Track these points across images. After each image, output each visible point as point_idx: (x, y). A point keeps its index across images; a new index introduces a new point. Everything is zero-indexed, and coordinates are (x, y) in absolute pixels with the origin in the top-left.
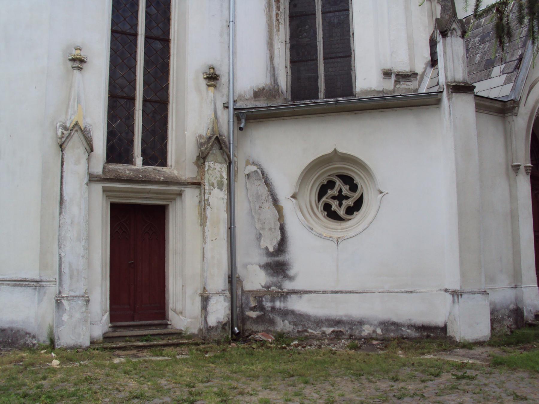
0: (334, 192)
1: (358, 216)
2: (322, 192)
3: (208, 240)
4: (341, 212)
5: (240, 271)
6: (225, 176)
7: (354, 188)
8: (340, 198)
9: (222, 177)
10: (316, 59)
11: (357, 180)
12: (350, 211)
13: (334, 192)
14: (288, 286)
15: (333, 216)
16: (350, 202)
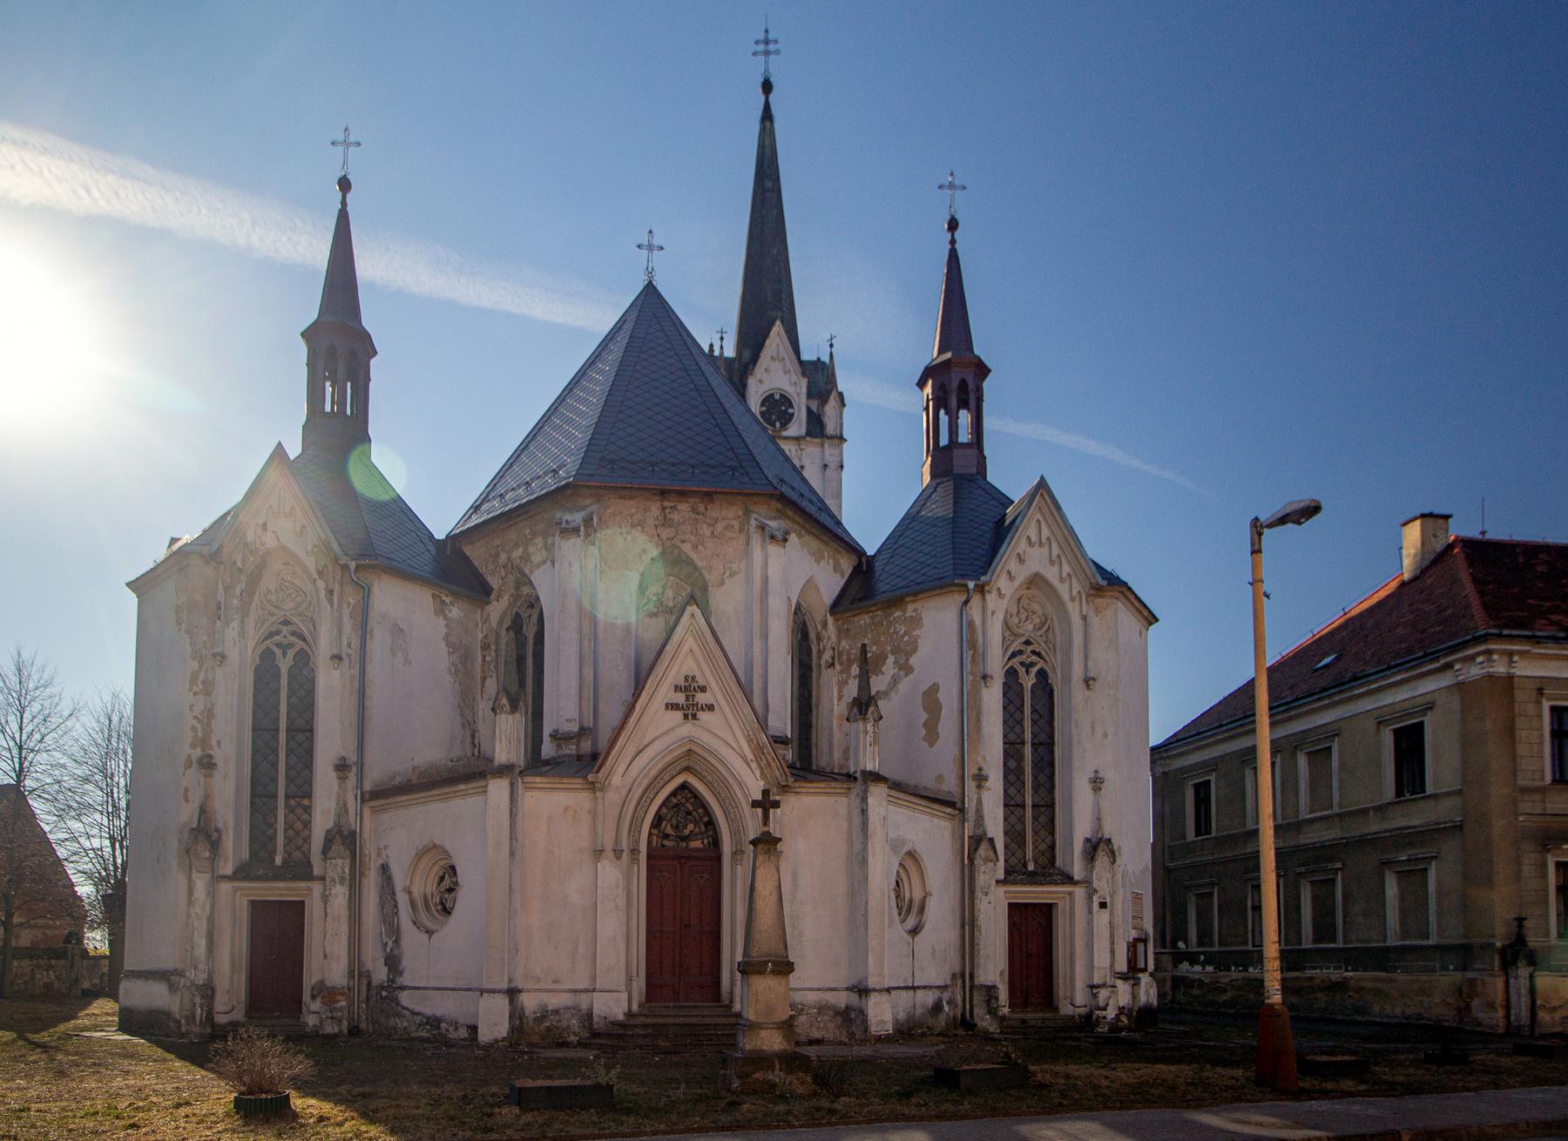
9: (344, 872)
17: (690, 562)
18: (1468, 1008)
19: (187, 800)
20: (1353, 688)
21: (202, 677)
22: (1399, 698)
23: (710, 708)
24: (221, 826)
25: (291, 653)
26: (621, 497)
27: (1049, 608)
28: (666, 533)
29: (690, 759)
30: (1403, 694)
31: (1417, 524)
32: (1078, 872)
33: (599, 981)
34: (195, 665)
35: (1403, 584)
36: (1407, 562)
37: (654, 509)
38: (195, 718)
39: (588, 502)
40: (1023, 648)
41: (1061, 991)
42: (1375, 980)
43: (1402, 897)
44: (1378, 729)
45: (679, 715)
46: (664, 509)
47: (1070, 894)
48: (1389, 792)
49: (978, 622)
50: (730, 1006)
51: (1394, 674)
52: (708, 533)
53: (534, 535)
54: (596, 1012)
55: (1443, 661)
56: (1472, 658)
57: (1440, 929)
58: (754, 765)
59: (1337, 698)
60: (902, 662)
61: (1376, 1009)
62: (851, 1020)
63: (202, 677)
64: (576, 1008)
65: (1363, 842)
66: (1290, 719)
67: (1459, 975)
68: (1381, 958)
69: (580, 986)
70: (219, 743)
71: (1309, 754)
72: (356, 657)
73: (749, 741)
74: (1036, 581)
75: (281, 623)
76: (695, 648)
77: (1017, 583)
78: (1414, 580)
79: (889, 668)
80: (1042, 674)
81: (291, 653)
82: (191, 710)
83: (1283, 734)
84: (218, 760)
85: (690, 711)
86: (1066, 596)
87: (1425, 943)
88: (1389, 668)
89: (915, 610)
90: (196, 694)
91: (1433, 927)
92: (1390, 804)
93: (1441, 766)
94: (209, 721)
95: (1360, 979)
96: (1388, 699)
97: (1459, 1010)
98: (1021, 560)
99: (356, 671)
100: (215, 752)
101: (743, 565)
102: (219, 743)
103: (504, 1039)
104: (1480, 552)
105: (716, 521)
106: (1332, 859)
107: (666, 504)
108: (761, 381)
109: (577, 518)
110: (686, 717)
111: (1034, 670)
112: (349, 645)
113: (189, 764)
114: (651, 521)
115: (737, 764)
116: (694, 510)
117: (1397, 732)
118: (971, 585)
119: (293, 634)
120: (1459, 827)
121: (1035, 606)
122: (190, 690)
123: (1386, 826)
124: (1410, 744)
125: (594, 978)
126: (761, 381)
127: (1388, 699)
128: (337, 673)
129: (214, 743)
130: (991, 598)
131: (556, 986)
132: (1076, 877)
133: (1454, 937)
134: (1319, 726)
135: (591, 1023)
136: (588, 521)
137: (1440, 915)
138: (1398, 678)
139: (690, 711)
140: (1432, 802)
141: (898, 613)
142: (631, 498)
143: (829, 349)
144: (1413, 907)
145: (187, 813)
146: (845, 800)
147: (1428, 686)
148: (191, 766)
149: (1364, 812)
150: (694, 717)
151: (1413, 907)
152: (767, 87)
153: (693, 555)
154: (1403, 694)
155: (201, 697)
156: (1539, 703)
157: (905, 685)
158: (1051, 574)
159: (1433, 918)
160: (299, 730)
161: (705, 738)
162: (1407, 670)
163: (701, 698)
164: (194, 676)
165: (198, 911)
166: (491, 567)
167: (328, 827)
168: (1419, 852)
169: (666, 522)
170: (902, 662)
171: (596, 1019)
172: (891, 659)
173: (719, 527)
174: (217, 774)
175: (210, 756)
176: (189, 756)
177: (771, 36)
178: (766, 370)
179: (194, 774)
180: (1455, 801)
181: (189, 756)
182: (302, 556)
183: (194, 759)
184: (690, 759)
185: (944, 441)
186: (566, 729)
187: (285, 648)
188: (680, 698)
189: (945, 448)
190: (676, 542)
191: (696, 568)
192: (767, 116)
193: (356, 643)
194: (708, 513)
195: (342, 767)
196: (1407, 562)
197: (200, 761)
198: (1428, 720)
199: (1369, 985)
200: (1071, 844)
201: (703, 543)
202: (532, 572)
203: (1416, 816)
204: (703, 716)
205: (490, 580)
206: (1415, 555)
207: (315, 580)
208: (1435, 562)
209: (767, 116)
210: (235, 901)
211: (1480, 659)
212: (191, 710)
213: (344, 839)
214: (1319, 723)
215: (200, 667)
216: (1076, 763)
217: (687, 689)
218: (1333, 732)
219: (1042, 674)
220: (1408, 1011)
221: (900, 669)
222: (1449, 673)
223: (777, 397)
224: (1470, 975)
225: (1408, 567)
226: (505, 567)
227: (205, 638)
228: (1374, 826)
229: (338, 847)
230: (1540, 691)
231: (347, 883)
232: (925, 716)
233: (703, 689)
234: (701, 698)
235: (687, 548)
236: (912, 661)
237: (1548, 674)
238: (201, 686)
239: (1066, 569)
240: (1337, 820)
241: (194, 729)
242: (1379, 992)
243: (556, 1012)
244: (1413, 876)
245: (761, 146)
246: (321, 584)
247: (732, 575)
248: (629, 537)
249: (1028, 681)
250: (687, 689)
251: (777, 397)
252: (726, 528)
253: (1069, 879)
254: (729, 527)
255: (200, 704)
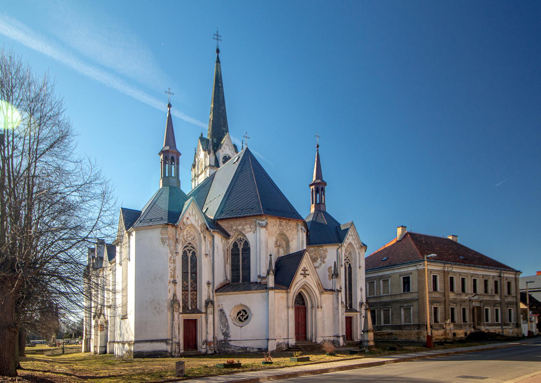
0: (241, 314)
1: (247, 320)
2: (238, 314)
3: (208, 328)
4: (243, 319)
5: (216, 335)
6: (212, 311)
7: (246, 313)
8: (243, 316)
10: (239, 270)
11: (247, 311)
12: (245, 319)
13: (241, 314)
14: (229, 339)
15: (241, 320)
16: (245, 317)
17: (285, 235)
18: (420, 337)
19: (170, 292)
20: (395, 267)
21: (172, 258)
22: (404, 271)
23: (308, 275)
24: (179, 299)
25: (191, 252)
26: (272, 218)
27: (351, 250)
28: (281, 228)
29: (305, 287)
30: (405, 270)
31: (401, 228)
32: (358, 309)
33: (289, 336)
34: (170, 255)
35: (397, 241)
36: (398, 236)
37: (278, 222)
38: (171, 270)
39: (264, 219)
40: (346, 258)
41: (354, 335)
42: (399, 332)
43: (405, 314)
44: (400, 277)
45: (303, 276)
46: (280, 222)
47: (356, 314)
48: (402, 291)
49: (340, 253)
50: (311, 340)
51: (404, 265)
52: (289, 229)
53: (247, 224)
54: (289, 343)
55: (415, 264)
56: (421, 265)
57: (414, 321)
58: (317, 288)
59: (391, 269)
60: (322, 260)
61: (399, 338)
62: (334, 343)
63: (172, 258)
64: (285, 343)
65: (397, 302)
66: (379, 272)
67: (417, 331)
68: (400, 327)
69: (285, 338)
70: (177, 276)
71: (383, 281)
72: (211, 255)
73: (316, 282)
74: (350, 244)
75: (188, 244)
76: (306, 261)
77: (347, 244)
78: (400, 241)
79: (319, 261)
80: (350, 265)
81: (191, 252)
82: (170, 267)
83: (377, 275)
84: (177, 281)
85: (305, 275)
86: (355, 248)
87: (410, 324)
88: (403, 264)
89: (326, 248)
90: (171, 263)
91: (412, 321)
92: (402, 293)
93: (414, 286)
94: (175, 271)
95: (395, 332)
96: (402, 270)
97: (418, 338)
98: (348, 239)
99: (211, 258)
100: (176, 279)
101: (296, 236)
102: (177, 276)
103: (275, 350)
104: (413, 236)
105: (291, 226)
106: (389, 305)
107: (281, 221)
108: (223, 151)
109: (264, 223)
110: (304, 276)
111: (348, 263)
112: (209, 251)
113: (170, 282)
114: (277, 225)
115: (314, 287)
116: (286, 223)
117: (403, 278)
118: (340, 244)
119: (191, 247)
120: (418, 300)
121: (348, 249)
122: (170, 262)
123: (402, 298)
124: (407, 281)
125: (288, 335)
126: (223, 151)
127: (402, 270)
128: (206, 259)
129: (176, 277)
130: (343, 247)
131: (280, 338)
132: (358, 311)
133: (417, 322)
134: (386, 275)
135: (288, 346)
136: (267, 224)
137: (413, 318)
138: (405, 266)
139: (305, 275)
140: (411, 294)
141: (321, 248)
142: (273, 218)
143: (242, 144)
144: (407, 316)
145: (170, 296)
146: (332, 295)
147: (411, 269)
148: (170, 283)
149: (397, 295)
150: (306, 277)
151: (407, 316)
152: (218, 51)
153: (286, 233)
154: (405, 270)
155: (172, 264)
156: (431, 275)
157: (323, 265)
158: (353, 242)
159: (412, 318)
160: (193, 273)
161: (308, 282)
162: (407, 265)
163: (307, 272)
164: (171, 258)
165: (176, 322)
166: (229, 229)
167: (206, 299)
168: (409, 304)
169: (280, 225)
170: (322, 260)
171: (289, 345)
172: (319, 259)
173: (291, 227)
174: (177, 285)
175: (175, 280)
176: (170, 280)
177: (219, 34)
178: (224, 148)
179: (171, 285)
180: (416, 294)
181: (170, 280)
182: (196, 226)
183: (171, 281)
184: (305, 287)
185: (318, 202)
186: (263, 276)
187: (190, 250)
188: (303, 272)
189: (318, 204)
190: (283, 230)
191: (286, 236)
192: (218, 61)
193: (211, 251)
194: (289, 223)
195: (208, 284)
196: (398, 236)
197: (173, 282)
198: (411, 276)
199: (398, 333)
200: (357, 303)
201: (288, 231)
202: (246, 233)
203: (408, 297)
204: (307, 276)
205: (229, 233)
206: (400, 235)
207: (200, 234)
208: (404, 237)
209: (218, 61)
210: (180, 318)
211: (422, 265)
212: (170, 267)
213: (209, 302)
214: (386, 274)
215: (172, 256)
216: (358, 285)
217: (304, 270)
218: (389, 276)
219: (350, 265)
220: (407, 339)
221: (322, 261)
222: (416, 267)
223: (227, 157)
224: (420, 330)
225: (398, 237)
226: (235, 230)
227: (173, 248)
228: (399, 298)
229: (210, 305)
230: (431, 272)
231: (213, 314)
232: (328, 273)
233: (307, 270)
234: (307, 272)
235: (285, 232)
236: (325, 260)
237: (432, 268)
238: (172, 261)
239: (356, 242)
240: (390, 296)
241: (171, 273)
242: (400, 335)
243: (281, 344)
244: (408, 309)
245: (217, 71)
246: (202, 235)
247: (294, 239)
248: (273, 228)
249: (347, 266)
250: (304, 270)
251: (227, 157)
252: (293, 227)
253: (356, 311)
254: (293, 227)
255: (172, 266)
